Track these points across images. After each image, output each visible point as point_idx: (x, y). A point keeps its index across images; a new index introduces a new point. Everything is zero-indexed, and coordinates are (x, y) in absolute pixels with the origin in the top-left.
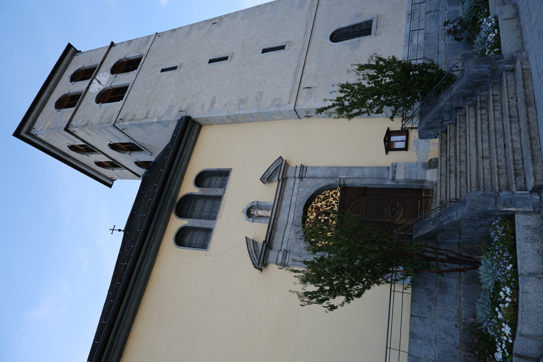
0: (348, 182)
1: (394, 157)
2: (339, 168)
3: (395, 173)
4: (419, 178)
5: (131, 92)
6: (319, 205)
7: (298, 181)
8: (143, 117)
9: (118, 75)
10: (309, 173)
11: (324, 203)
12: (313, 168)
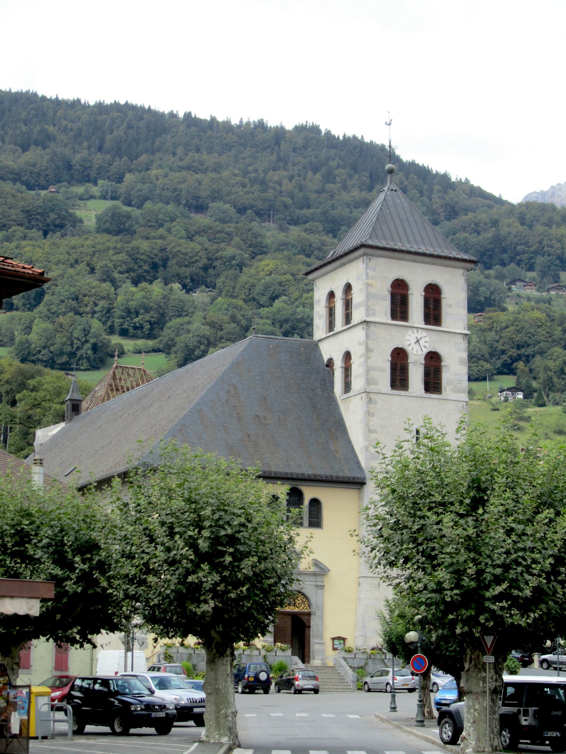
0: (312, 617)
1: (329, 644)
2: (322, 610)
3: (319, 643)
4: (316, 657)
5: (399, 397)
6: (299, 598)
7: (314, 583)
8: (370, 427)
9: (423, 367)
10: (320, 591)
11: (300, 602)
12: (323, 593)
